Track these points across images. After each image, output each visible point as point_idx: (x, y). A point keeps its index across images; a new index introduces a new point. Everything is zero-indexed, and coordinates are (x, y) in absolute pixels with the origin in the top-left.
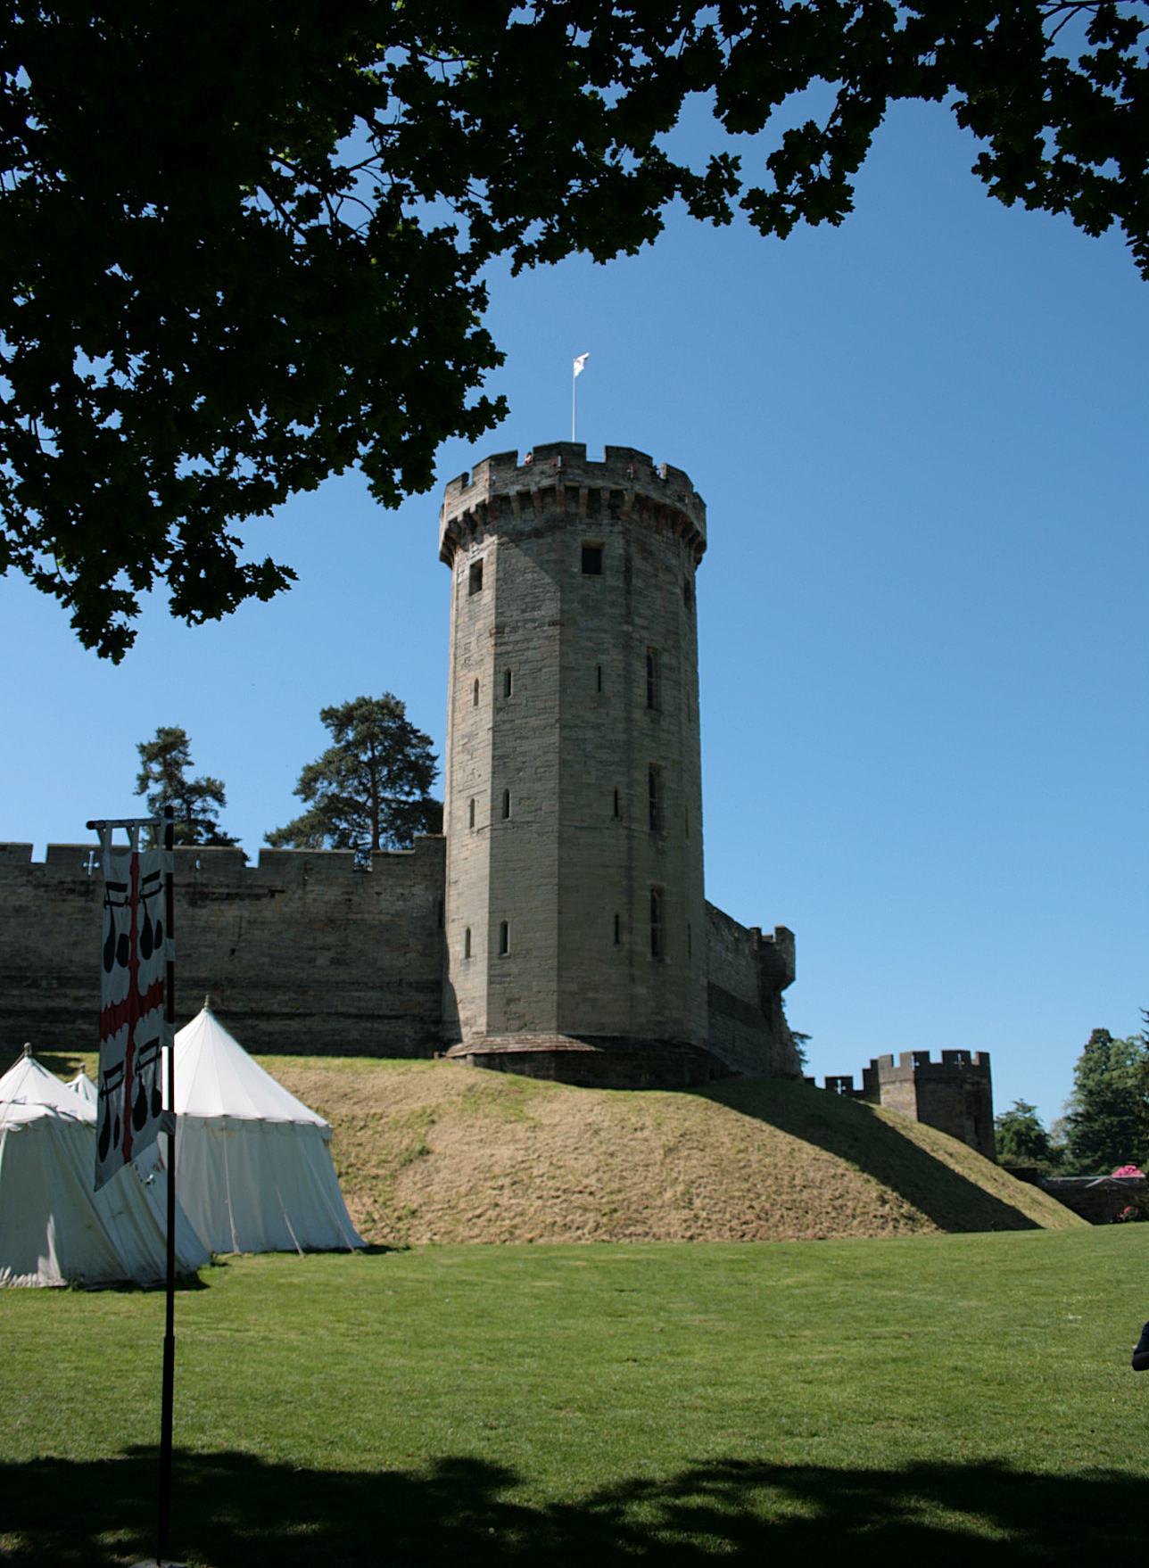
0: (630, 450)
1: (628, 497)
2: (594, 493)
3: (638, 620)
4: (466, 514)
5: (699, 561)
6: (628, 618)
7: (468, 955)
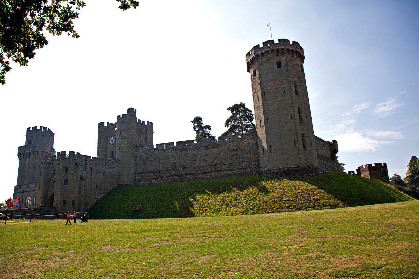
0: (284, 39)
1: (286, 49)
2: (277, 50)
3: (291, 76)
4: (251, 60)
5: (303, 61)
6: (289, 76)
7: (264, 153)
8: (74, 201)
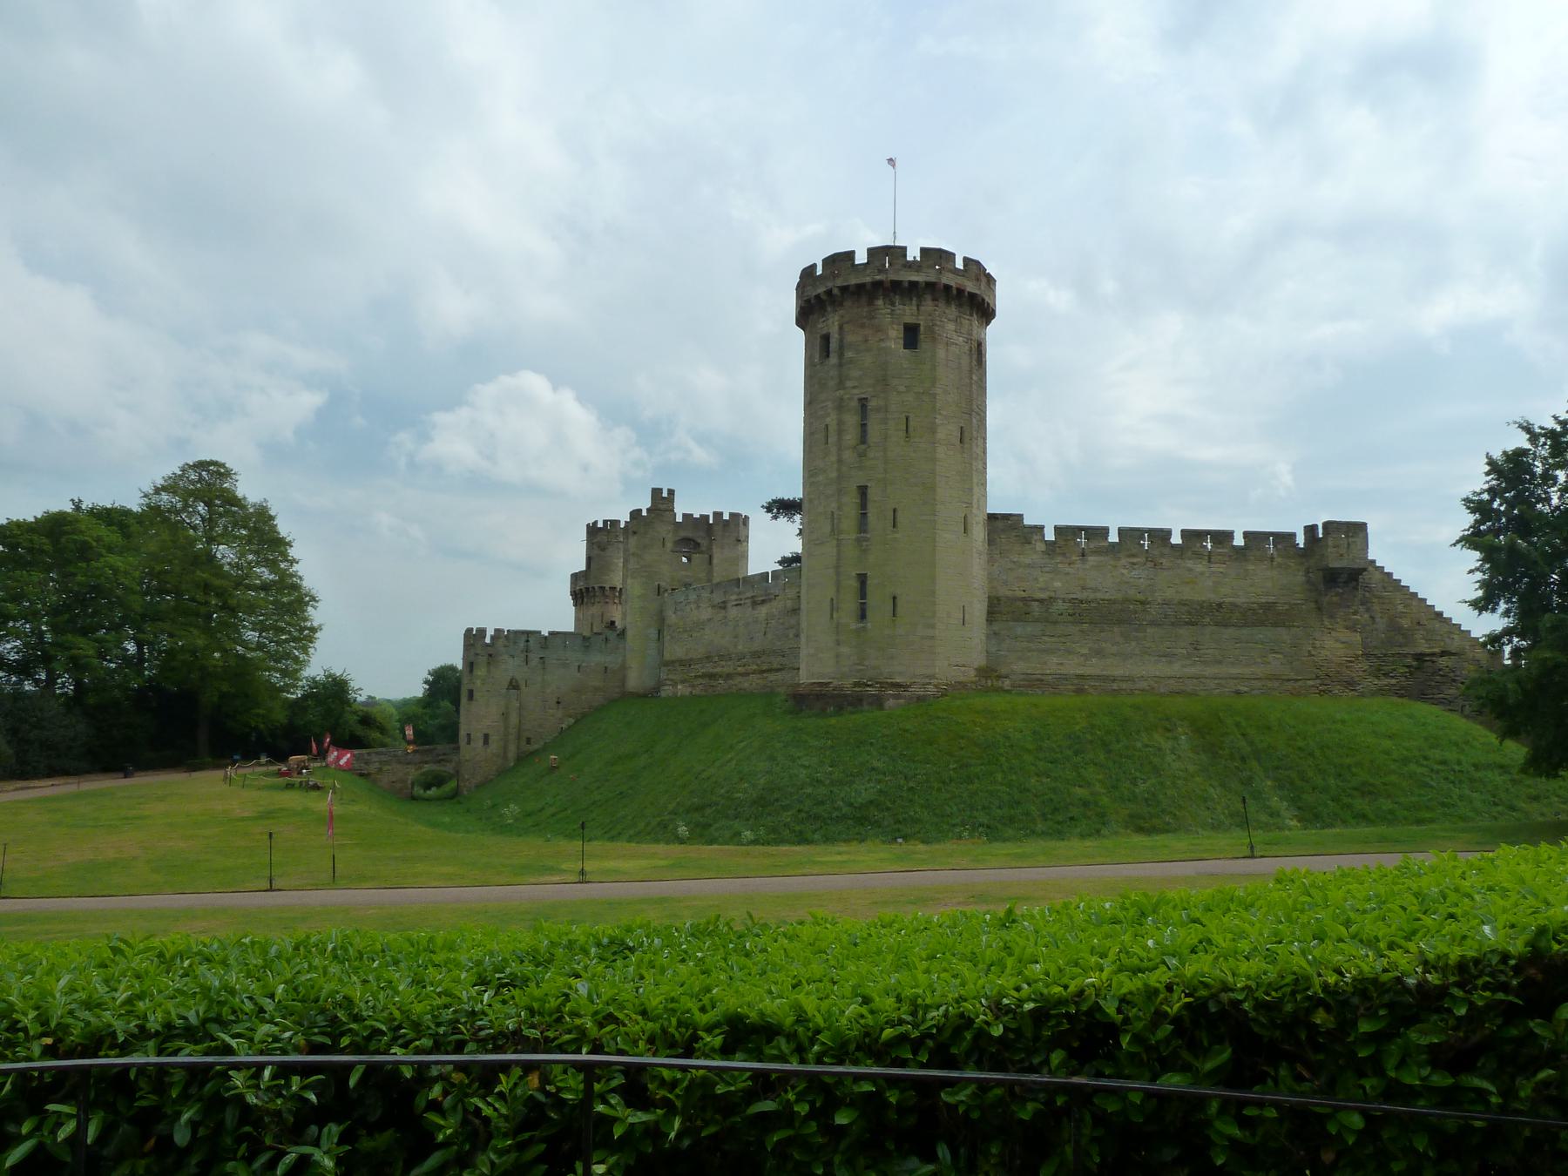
1: (836, 291)
6: (841, 384)
8: (486, 737)
